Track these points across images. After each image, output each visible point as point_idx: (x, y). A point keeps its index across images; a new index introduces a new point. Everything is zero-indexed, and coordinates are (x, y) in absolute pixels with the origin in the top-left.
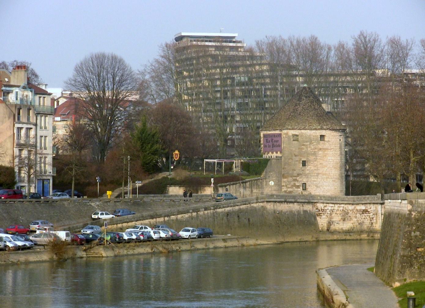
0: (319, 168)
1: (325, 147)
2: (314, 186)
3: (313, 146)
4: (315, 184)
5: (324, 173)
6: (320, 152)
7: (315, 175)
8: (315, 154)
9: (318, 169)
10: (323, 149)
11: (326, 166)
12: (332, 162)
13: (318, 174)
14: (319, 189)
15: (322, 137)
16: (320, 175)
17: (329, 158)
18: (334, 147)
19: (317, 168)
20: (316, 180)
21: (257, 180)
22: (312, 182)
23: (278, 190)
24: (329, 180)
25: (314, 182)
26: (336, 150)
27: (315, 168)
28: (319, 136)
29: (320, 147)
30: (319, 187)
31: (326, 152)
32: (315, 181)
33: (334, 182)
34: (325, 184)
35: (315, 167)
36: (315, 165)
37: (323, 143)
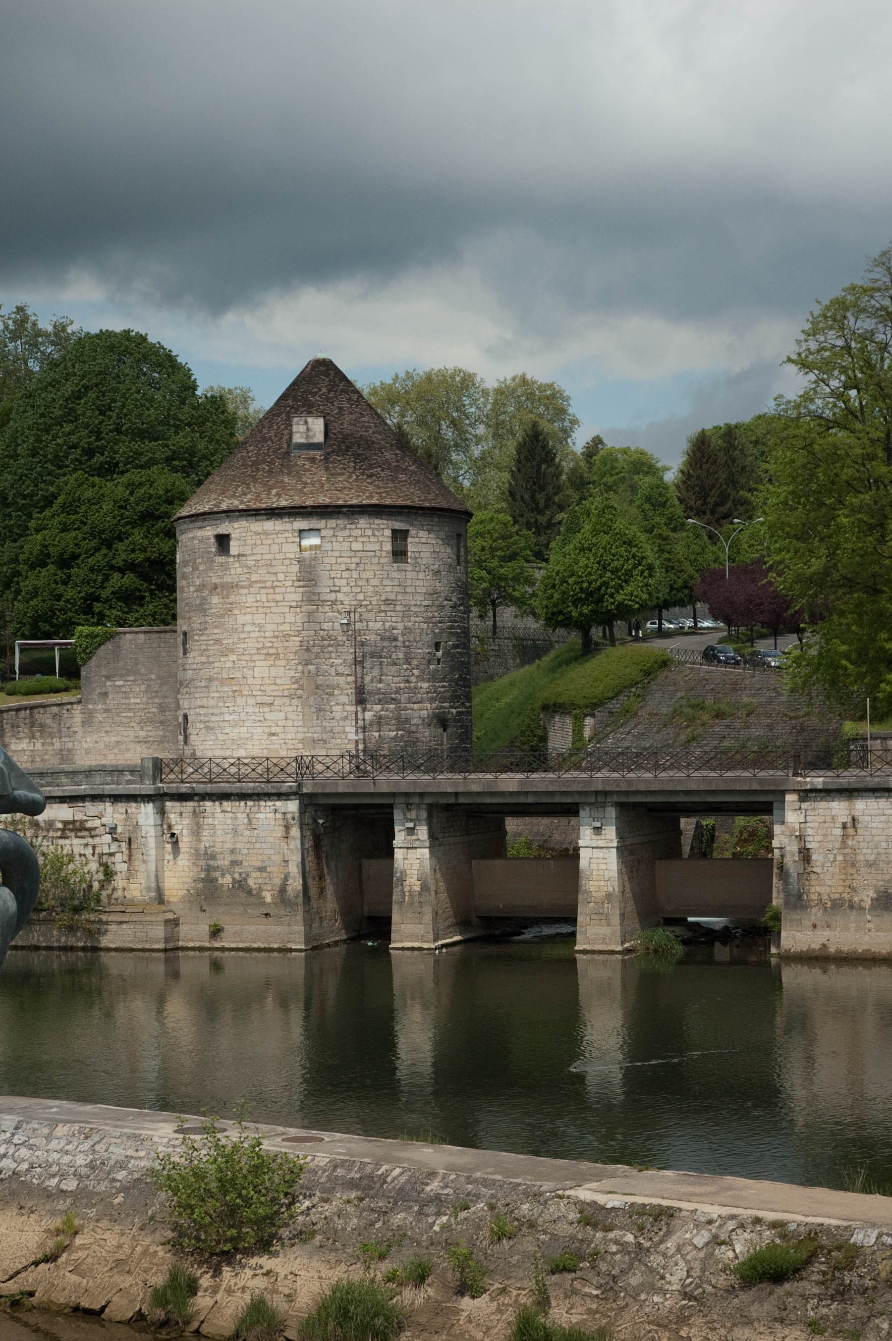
0: (211, 659)
1: (227, 579)
2: (202, 726)
3: (199, 578)
4: (202, 718)
5: (225, 676)
6: (215, 600)
7: (203, 684)
8: (202, 608)
9: (209, 663)
10: (223, 586)
11: (232, 651)
12: (252, 635)
13: (210, 679)
14: (213, 738)
15: (223, 541)
16: (215, 683)
17: (241, 619)
18: (267, 577)
19: (208, 657)
20: (204, 702)
21: (32, 708)
22: (198, 710)
23: (161, 742)
24: (240, 701)
25: (203, 711)
26: (273, 587)
27: (204, 659)
28: (213, 540)
29: (215, 580)
30: (212, 729)
31: (232, 598)
32: (203, 707)
33: (267, 709)
34: (227, 718)
35: (202, 656)
36: (204, 647)
37: (222, 565)
